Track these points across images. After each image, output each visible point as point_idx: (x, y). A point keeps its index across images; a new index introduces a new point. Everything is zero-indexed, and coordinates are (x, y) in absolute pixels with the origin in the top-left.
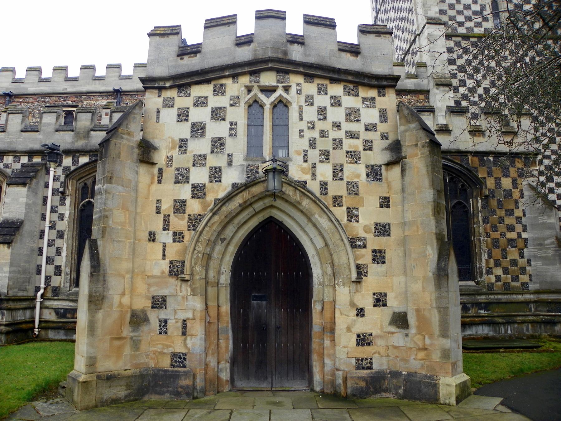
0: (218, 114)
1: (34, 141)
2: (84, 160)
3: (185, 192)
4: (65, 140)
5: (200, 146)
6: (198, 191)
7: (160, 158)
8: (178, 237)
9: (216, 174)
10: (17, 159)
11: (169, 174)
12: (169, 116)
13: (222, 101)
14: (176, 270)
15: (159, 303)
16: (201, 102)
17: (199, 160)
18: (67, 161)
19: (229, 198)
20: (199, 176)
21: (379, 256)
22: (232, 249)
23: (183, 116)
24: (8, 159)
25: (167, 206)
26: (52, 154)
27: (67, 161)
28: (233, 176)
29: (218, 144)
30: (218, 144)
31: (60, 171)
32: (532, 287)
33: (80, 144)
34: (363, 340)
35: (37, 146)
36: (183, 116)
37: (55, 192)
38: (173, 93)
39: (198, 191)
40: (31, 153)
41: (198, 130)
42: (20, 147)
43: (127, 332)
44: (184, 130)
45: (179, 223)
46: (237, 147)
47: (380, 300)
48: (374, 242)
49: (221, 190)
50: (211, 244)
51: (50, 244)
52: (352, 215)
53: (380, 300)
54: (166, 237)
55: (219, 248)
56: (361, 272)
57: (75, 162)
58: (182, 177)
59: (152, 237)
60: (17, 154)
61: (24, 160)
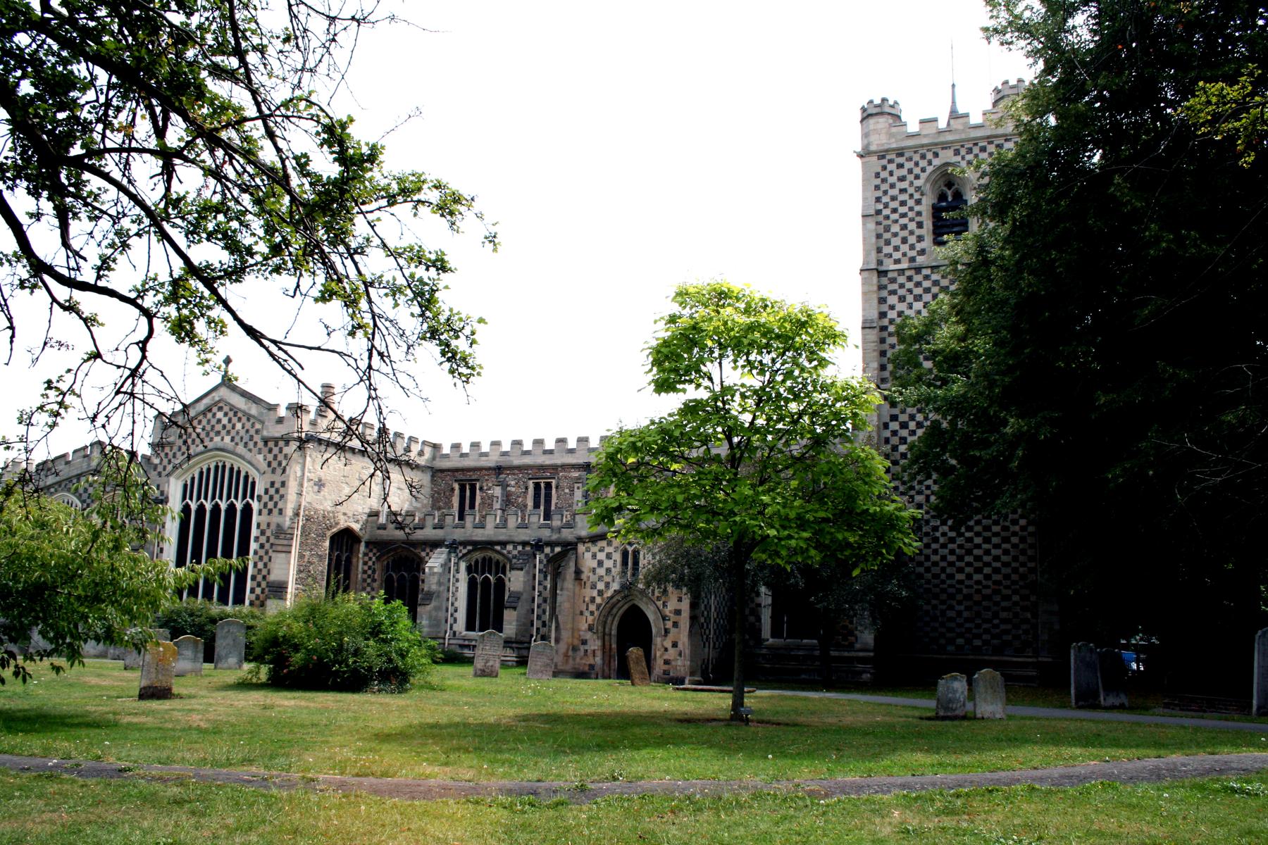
0: (609, 556)
1: (524, 535)
2: (558, 549)
3: (595, 593)
4: (546, 534)
5: (601, 571)
6: (600, 593)
7: (584, 577)
8: (592, 613)
9: (607, 585)
10: (515, 548)
11: (588, 585)
12: (588, 555)
13: (610, 549)
14: (590, 628)
15: (584, 642)
16: (601, 550)
17: (601, 578)
18: (547, 550)
19: (612, 597)
20: (601, 586)
21: (675, 624)
22: (617, 619)
23: (594, 556)
24: (510, 547)
25: (587, 599)
26: (538, 546)
27: (547, 550)
28: (615, 586)
29: (608, 571)
30: (608, 571)
31: (543, 556)
32: (858, 646)
33: (555, 537)
34: (667, 662)
35: (526, 538)
36: (594, 556)
37: (540, 571)
38: (590, 545)
39: (600, 593)
40: (524, 544)
41: (600, 563)
42: (517, 539)
43: (570, 653)
44: (594, 564)
45: (593, 607)
46: (616, 571)
47: (675, 645)
48: (673, 618)
49: (609, 593)
50: (606, 617)
51: (539, 607)
52: (665, 605)
53: (675, 645)
54: (587, 614)
55: (610, 618)
56: (667, 631)
57: (552, 551)
58: (594, 586)
59: (582, 613)
60: (515, 544)
61: (520, 548)
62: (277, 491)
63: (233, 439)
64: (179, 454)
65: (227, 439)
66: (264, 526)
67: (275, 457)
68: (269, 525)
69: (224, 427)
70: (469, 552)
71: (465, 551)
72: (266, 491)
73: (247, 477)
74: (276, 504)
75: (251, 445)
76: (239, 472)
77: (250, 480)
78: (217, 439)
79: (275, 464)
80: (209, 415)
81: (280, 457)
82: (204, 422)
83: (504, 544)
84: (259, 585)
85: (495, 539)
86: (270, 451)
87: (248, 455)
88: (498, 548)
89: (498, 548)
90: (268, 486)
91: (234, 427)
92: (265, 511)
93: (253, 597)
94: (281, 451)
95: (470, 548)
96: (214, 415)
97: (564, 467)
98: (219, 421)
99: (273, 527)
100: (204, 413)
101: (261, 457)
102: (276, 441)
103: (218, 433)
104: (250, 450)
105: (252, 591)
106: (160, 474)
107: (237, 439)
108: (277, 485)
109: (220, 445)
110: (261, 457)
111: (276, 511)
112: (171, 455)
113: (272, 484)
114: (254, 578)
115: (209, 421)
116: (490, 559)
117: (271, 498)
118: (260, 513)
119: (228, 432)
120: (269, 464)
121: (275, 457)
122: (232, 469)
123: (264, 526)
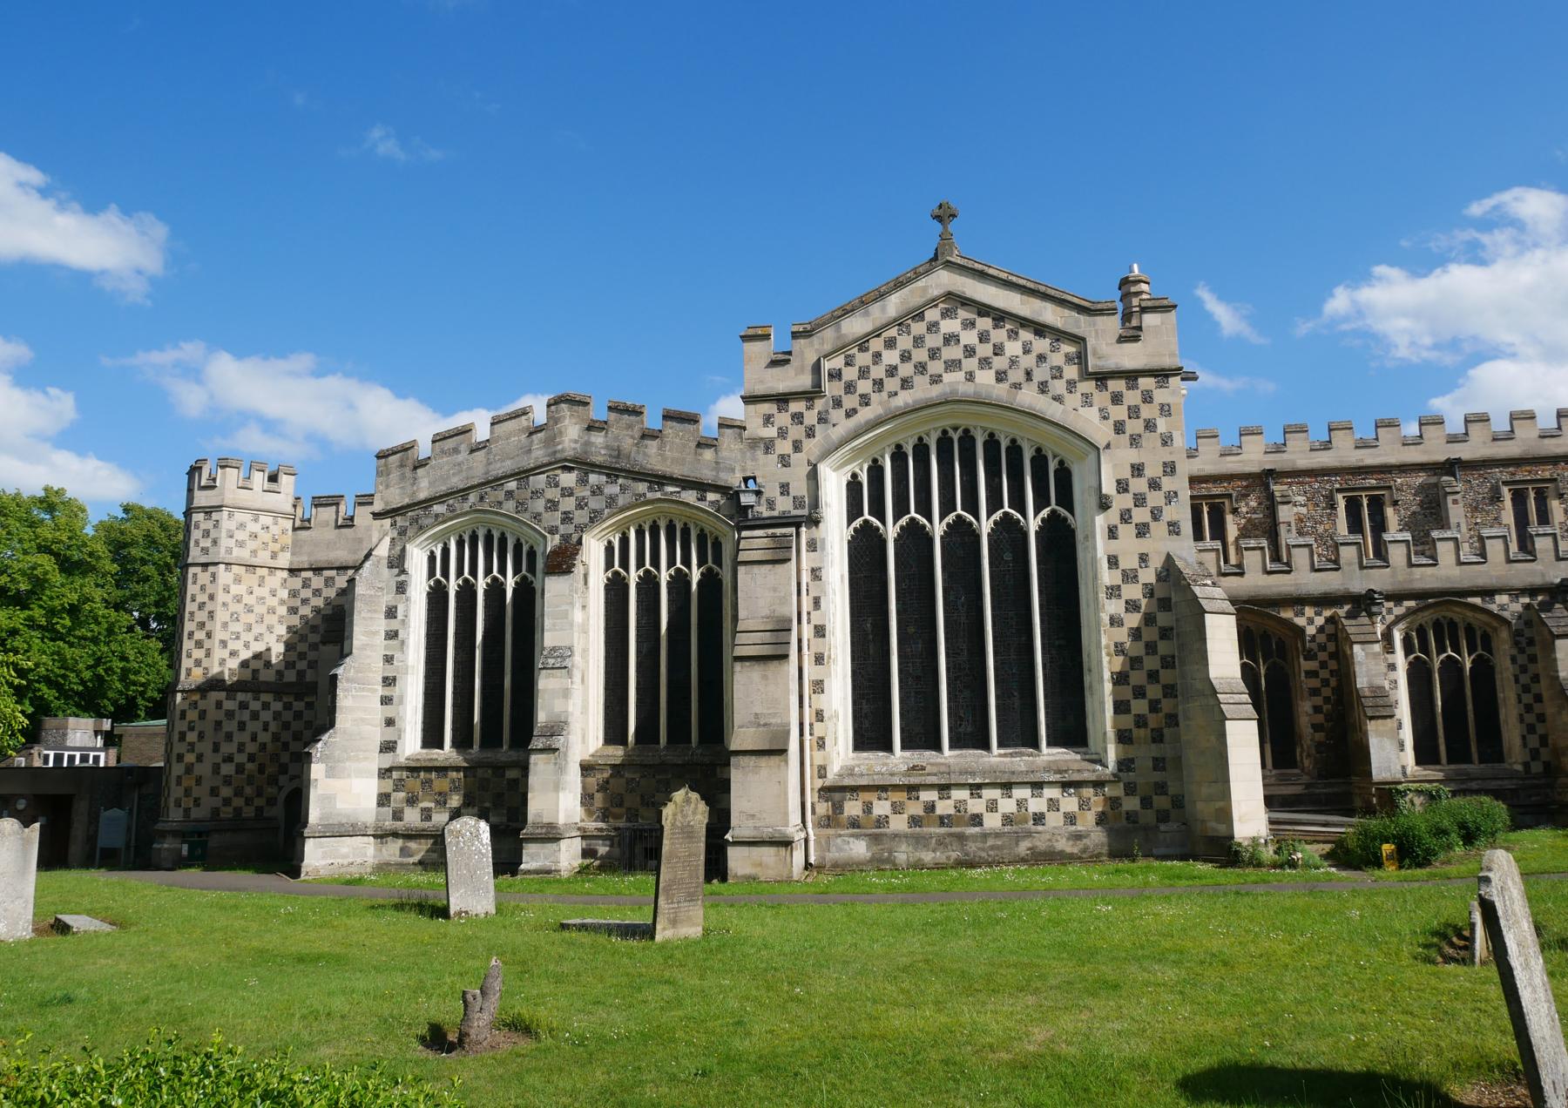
35: (1538, 581)
40: (1532, 591)
42: (1518, 582)
60: (1515, 593)
62: (1154, 485)
63: (1001, 377)
64: (837, 415)
65: (986, 378)
66: (1129, 562)
67: (1134, 412)
68: (1143, 558)
69: (970, 351)
70: (1410, 612)
71: (1399, 611)
72: (1122, 487)
73: (1040, 460)
74: (1156, 514)
75: (1059, 387)
76: (1015, 450)
77: (1052, 466)
78: (954, 379)
79: (1134, 426)
80: (918, 328)
81: (1147, 412)
82: (905, 342)
83: (1488, 593)
84: (1139, 693)
85: (1466, 584)
86: (1117, 399)
87: (1054, 411)
88: (1477, 601)
89: (1477, 601)
90: (1126, 473)
91: (998, 350)
92: (1127, 531)
93: (1128, 721)
94: (1147, 398)
95: (1412, 603)
96: (933, 327)
97: (1404, 469)
98: (950, 339)
99: (1156, 562)
100: (900, 322)
101: (1092, 414)
102: (1131, 376)
103: (953, 365)
104: (1058, 399)
105: (1120, 707)
106: (784, 461)
107: (1016, 376)
108: (1153, 470)
109: (966, 389)
110: (1092, 414)
111: (1159, 529)
112: (811, 418)
113: (1137, 470)
114: (1120, 679)
115: (918, 341)
116: (1452, 624)
117: (1140, 500)
118: (1112, 533)
119: (985, 363)
120: (1119, 428)
121: (1134, 412)
122: (992, 444)
123: (1129, 562)
